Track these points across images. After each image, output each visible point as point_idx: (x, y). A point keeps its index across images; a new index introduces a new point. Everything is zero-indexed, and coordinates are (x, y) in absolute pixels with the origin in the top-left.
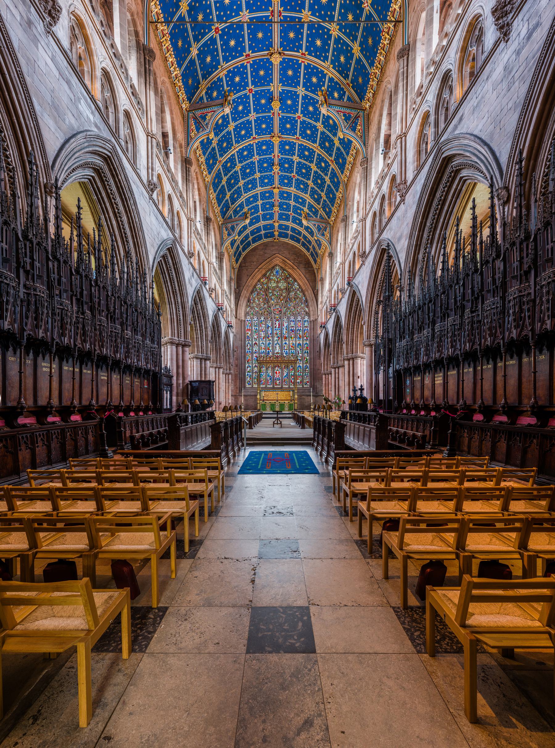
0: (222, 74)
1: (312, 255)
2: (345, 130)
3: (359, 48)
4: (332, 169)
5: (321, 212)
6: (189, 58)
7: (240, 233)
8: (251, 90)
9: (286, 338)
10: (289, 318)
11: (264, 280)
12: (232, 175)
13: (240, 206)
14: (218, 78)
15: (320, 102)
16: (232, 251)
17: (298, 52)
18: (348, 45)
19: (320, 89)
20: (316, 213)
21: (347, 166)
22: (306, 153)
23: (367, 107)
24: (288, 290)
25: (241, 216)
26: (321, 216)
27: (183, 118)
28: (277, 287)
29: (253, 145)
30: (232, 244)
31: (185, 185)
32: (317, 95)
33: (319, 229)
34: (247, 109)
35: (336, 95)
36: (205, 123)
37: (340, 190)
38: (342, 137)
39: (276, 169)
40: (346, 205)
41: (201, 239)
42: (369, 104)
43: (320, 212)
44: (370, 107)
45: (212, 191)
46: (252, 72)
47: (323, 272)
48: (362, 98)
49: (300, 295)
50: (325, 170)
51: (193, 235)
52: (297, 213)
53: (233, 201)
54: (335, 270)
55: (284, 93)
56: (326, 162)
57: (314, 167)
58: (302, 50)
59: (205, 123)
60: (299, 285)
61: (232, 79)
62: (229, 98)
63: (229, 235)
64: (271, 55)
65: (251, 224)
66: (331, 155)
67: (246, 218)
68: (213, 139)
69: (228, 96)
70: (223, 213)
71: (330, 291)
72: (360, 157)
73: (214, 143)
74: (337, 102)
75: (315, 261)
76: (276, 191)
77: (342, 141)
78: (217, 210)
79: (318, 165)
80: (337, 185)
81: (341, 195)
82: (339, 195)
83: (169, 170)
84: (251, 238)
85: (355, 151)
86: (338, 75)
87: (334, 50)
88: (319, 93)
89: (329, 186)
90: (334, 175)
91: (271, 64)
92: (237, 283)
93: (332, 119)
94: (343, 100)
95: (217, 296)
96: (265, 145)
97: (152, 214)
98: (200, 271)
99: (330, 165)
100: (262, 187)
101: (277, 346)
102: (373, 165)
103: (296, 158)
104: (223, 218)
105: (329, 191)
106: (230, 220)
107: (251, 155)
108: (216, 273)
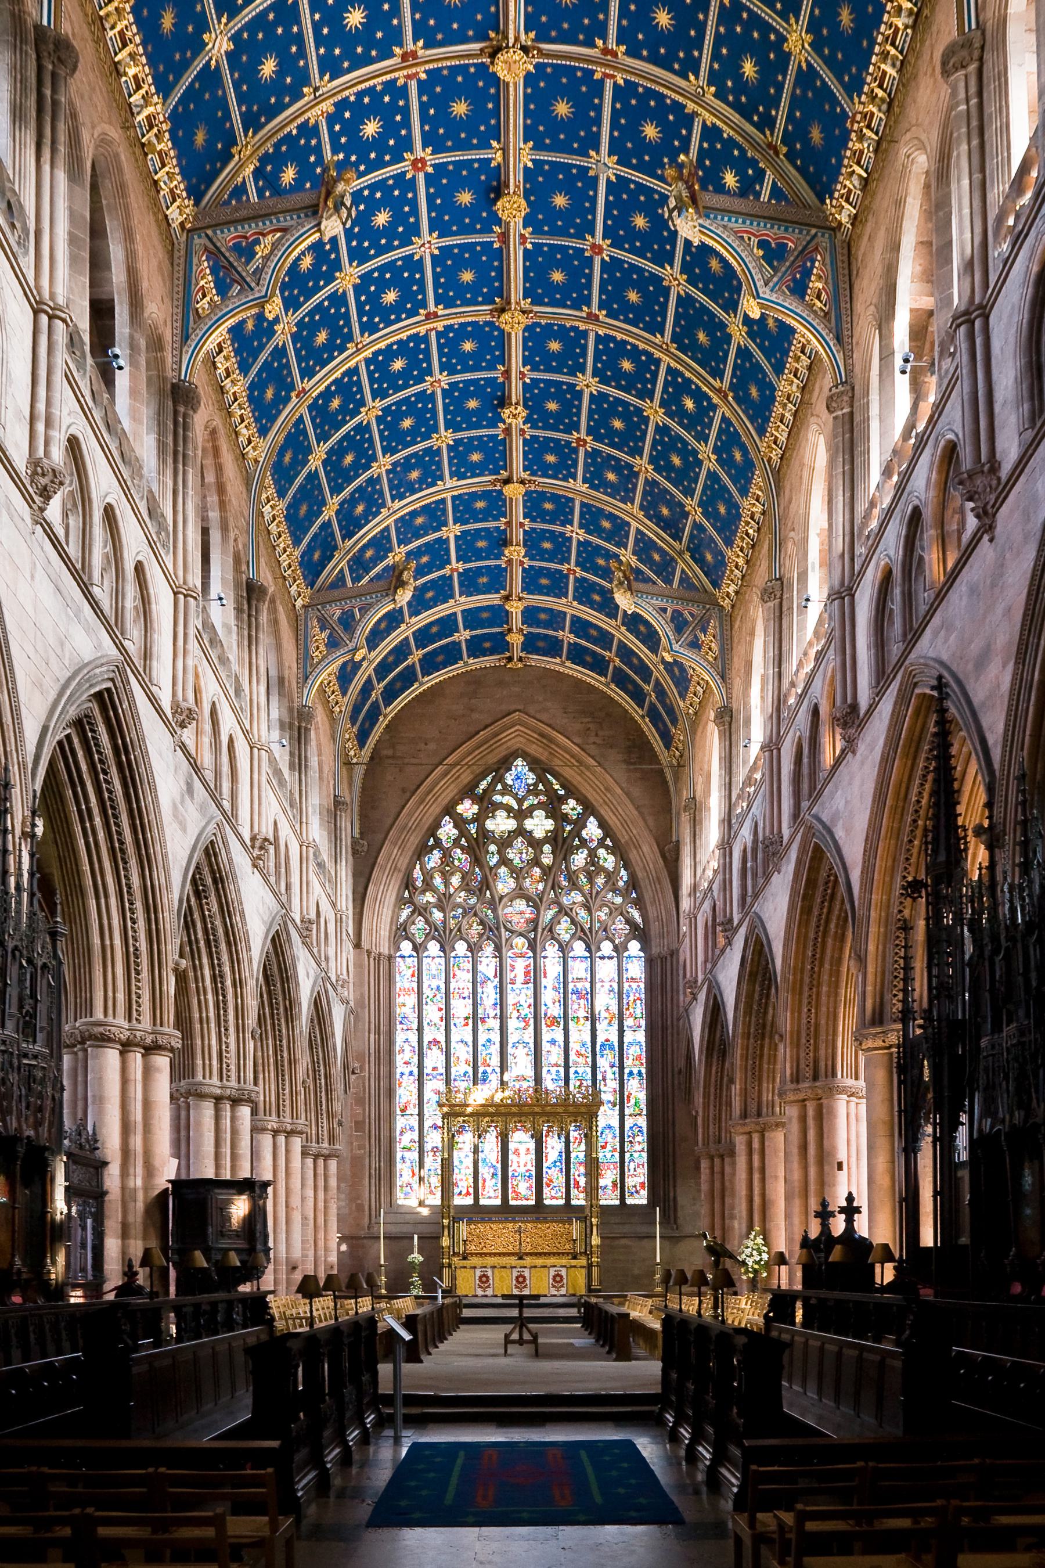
0: (317, 111)
1: (653, 715)
2: (765, 292)
3: (808, 38)
4: (724, 419)
5: (685, 565)
6: (198, 65)
7: (374, 639)
8: (423, 161)
11: (467, 808)
12: (346, 436)
13: (373, 543)
14: (303, 128)
15: (672, 203)
16: (344, 704)
17: (592, 45)
18: (766, 28)
19: (673, 160)
20: (665, 568)
21: (777, 409)
22: (627, 365)
23: (844, 218)
25: (378, 577)
26: (685, 580)
27: (171, 254)
29: (426, 339)
30: (345, 676)
31: (169, 472)
32: (662, 179)
33: (679, 624)
34: (404, 222)
35: (730, 179)
36: (252, 268)
37: (754, 489)
38: (755, 314)
39: (515, 416)
40: (778, 545)
41: (224, 660)
42: (849, 210)
43: (681, 565)
44: (854, 219)
45: (272, 491)
46: (423, 108)
47: (700, 780)
48: (823, 189)
49: (608, 861)
50: (698, 422)
51: (193, 645)
52: (595, 570)
53: (351, 524)
54: (741, 775)
55: (543, 173)
56: (699, 396)
57: (655, 413)
58: (604, 38)
59: (252, 268)
60: (603, 824)
61: (352, 128)
62: (340, 187)
63: (333, 644)
64: (493, 55)
65: (418, 604)
66: (717, 374)
67: (401, 584)
68: (277, 320)
69: (336, 181)
70: (311, 569)
71: (726, 846)
72: (825, 383)
73: (284, 333)
74: (737, 204)
75: (667, 739)
76: (514, 492)
77: (756, 328)
78: (290, 556)
79: (671, 404)
80: (743, 474)
81: (758, 509)
82: (750, 506)
83: (111, 424)
84: (416, 656)
85: (805, 361)
86: (736, 117)
87: (718, 40)
88: (670, 172)
89: (712, 476)
90: (729, 439)
91: (495, 80)
92: (364, 817)
93: (718, 254)
94: (758, 195)
95: (283, 866)
96: (469, 336)
97: (40, 573)
98: (217, 774)
99: (714, 407)
100: (462, 477)
102: (874, 410)
103: (588, 383)
104: (312, 584)
105: (715, 493)
106: (336, 593)
107: (418, 370)
108: (282, 782)
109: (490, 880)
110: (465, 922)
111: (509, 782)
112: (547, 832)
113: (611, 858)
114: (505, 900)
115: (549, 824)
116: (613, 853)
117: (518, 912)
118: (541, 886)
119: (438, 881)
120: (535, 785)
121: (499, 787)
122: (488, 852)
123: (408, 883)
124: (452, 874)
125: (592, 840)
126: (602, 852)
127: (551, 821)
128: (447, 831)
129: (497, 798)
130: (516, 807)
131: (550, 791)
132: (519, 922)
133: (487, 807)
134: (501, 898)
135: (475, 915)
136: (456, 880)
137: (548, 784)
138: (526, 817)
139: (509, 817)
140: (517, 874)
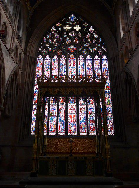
10: (85, 57)
11: (59, 24)
24: (84, 32)
28: (72, 29)
49: (96, 36)
109: (64, 40)
115: (80, 28)
116: (97, 34)
117: (72, 48)
118: (78, 42)
120: (76, 19)
122: (64, 34)
123: (42, 41)
124: (54, 39)
125: (91, 31)
126: (94, 34)
128: (54, 29)
129: (67, 22)
131: (80, 20)
132: (72, 51)
133: (64, 24)
139: (69, 26)
140: (72, 39)
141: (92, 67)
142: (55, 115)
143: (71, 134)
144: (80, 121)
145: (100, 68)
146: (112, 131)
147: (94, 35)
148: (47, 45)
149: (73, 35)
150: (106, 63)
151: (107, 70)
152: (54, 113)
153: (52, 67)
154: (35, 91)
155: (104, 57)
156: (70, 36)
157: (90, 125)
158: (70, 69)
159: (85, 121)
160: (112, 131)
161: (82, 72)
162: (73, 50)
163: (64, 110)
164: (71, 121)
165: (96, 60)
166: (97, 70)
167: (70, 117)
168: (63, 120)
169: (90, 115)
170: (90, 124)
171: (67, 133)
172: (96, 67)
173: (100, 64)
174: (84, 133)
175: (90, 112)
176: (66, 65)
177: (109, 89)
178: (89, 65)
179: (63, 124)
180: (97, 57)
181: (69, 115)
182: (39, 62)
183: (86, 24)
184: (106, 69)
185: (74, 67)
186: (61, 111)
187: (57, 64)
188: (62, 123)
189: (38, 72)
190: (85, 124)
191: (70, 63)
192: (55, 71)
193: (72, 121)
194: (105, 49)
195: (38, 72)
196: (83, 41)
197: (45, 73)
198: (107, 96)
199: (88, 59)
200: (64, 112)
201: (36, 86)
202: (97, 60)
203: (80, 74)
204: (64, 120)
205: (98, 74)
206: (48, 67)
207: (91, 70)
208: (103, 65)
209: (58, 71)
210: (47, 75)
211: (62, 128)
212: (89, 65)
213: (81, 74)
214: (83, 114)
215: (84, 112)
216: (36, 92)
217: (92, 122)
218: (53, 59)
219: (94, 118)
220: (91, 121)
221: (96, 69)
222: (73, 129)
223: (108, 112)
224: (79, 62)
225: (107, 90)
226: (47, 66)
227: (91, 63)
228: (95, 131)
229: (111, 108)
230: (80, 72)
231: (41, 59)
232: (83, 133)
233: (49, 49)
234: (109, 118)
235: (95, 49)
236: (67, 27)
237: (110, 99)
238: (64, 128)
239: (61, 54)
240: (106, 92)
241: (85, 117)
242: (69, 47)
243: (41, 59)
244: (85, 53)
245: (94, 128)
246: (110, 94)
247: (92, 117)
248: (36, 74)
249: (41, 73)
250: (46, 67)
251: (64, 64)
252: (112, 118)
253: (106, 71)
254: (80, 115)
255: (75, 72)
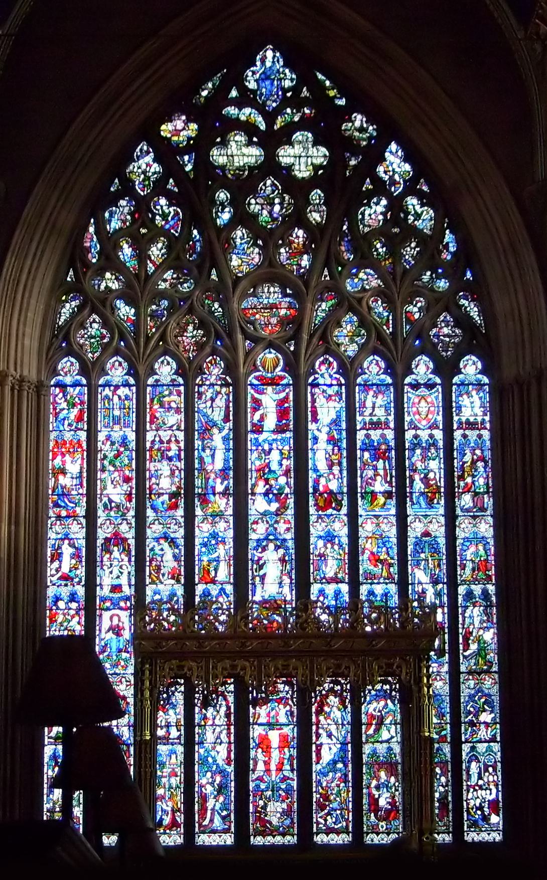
9: (330, 500)
101: (271, 556)
110: (173, 324)
111: (252, 85)
112: (316, 168)
113: (428, 214)
114: (243, 285)
115: (320, 155)
116: (430, 204)
118: (305, 261)
119: (126, 252)
120: (296, 89)
121: (234, 93)
122: (213, 202)
124: (153, 240)
125: (393, 182)
126: (412, 202)
127: (323, 150)
129: (232, 111)
130: (263, 127)
131: (319, 98)
134: (237, 281)
135: (191, 311)
136: (157, 251)
137: (318, 89)
138: (280, 144)
139: (250, 143)
141: (390, 434)
142: (174, 733)
143: (269, 838)
144: (319, 767)
145: (441, 444)
146: (494, 819)
147: (407, 213)
148: (111, 282)
149: (277, 208)
150: (479, 411)
151: (482, 459)
152: (168, 726)
153: (150, 436)
154: (51, 592)
155: (471, 367)
156: (255, 216)
157: (374, 792)
158: (255, 455)
159: (346, 766)
160: (494, 819)
161: (330, 467)
162: (274, 321)
163: (224, 709)
164: (268, 771)
165: (415, 386)
166: (424, 458)
167: (258, 746)
168: (220, 762)
169: (371, 732)
170: (374, 783)
171: (242, 833)
172: (416, 437)
173: (440, 418)
174: (338, 832)
175: (373, 717)
176: (230, 425)
177: (489, 578)
178: (376, 425)
179: (221, 789)
180: (423, 368)
181: (256, 732)
182: (64, 405)
183: (357, 124)
184: (478, 452)
185: (279, 436)
186: (210, 712)
187: (173, 419)
188: (218, 779)
189: (63, 472)
190: (346, 781)
191: (255, 410)
192: (165, 468)
193: (273, 767)
194: (474, 312)
195: (63, 472)
196: (339, 254)
197: (105, 475)
198: (477, 624)
199: (366, 387)
200: (228, 716)
201: (56, 564)
202: (423, 391)
203: (317, 482)
204: (229, 764)
205: (425, 480)
206: (124, 438)
207: (386, 458)
208: (460, 423)
209: (181, 465)
210: (119, 490)
211: (218, 806)
212: (376, 425)
213: (323, 481)
214: (333, 728)
215: (337, 714)
216: (57, 599)
217: (383, 774)
218: (150, 381)
219: (397, 749)
220: (381, 765)
221: (418, 452)
222: (275, 811)
223: (476, 715)
224: (314, 401)
225: (475, 581)
226: (117, 435)
227: (387, 409)
228: (398, 824)
229: (495, 690)
230: (316, 470)
231: (75, 385)
232: (332, 836)
233: (125, 311)
234: (482, 747)
235: (415, 310)
236: (233, 148)
237: (489, 636)
238: (225, 807)
239: (200, 346)
240: (469, 595)
241: (344, 744)
242: (252, 301)
243: (75, 385)
244: (352, 341)
245: (393, 803)
246: (491, 606)
247: (385, 745)
248: (51, 483)
249: (81, 477)
250: (108, 438)
251: (217, 416)
252: (496, 747)
253: (474, 462)
254: (318, 736)
255: (286, 473)
